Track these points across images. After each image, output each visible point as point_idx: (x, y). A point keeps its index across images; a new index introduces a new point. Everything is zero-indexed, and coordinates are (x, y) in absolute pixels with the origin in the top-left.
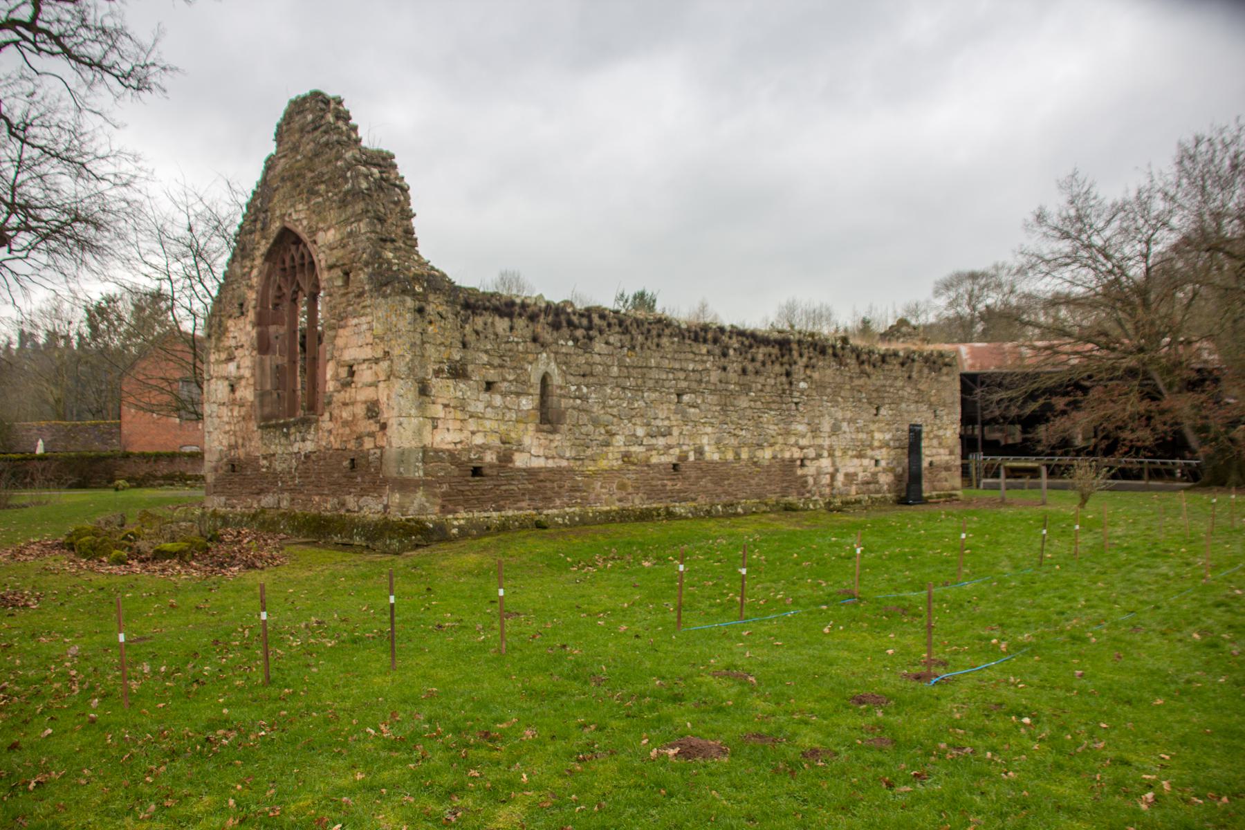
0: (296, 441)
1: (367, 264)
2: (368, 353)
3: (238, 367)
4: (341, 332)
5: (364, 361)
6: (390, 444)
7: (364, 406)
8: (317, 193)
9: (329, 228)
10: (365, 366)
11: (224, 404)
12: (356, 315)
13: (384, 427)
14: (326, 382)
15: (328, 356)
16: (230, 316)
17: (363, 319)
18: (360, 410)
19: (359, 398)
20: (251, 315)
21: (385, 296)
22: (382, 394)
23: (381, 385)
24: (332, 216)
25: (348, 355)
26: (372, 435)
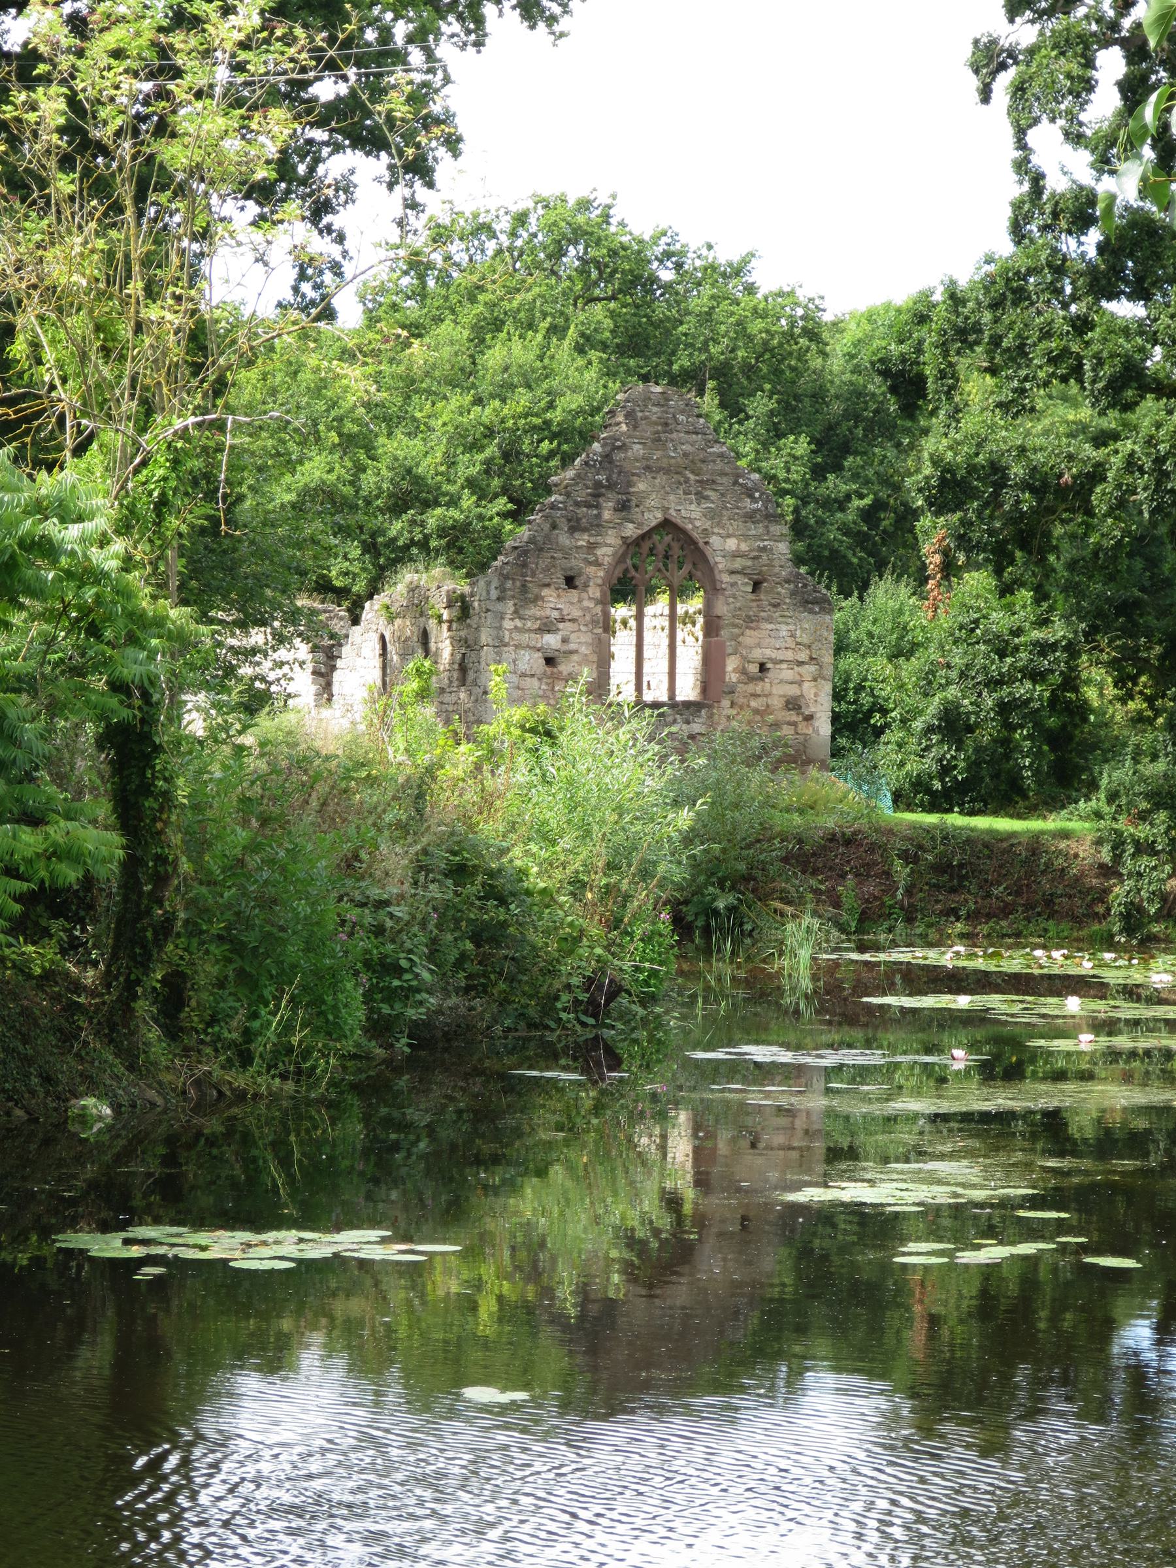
0: (675, 721)
1: (788, 581)
2: (789, 655)
3: (565, 641)
4: (748, 632)
5: (782, 661)
6: (817, 731)
7: (783, 700)
8: (707, 498)
9: (729, 536)
10: (784, 666)
11: (533, 676)
12: (769, 620)
13: (809, 718)
14: (724, 672)
15: (729, 650)
16: (548, 585)
17: (784, 627)
18: (777, 703)
19: (774, 691)
20: (595, 592)
21: (811, 612)
22: (808, 689)
23: (806, 685)
24: (735, 526)
25: (758, 654)
26: (794, 724)
